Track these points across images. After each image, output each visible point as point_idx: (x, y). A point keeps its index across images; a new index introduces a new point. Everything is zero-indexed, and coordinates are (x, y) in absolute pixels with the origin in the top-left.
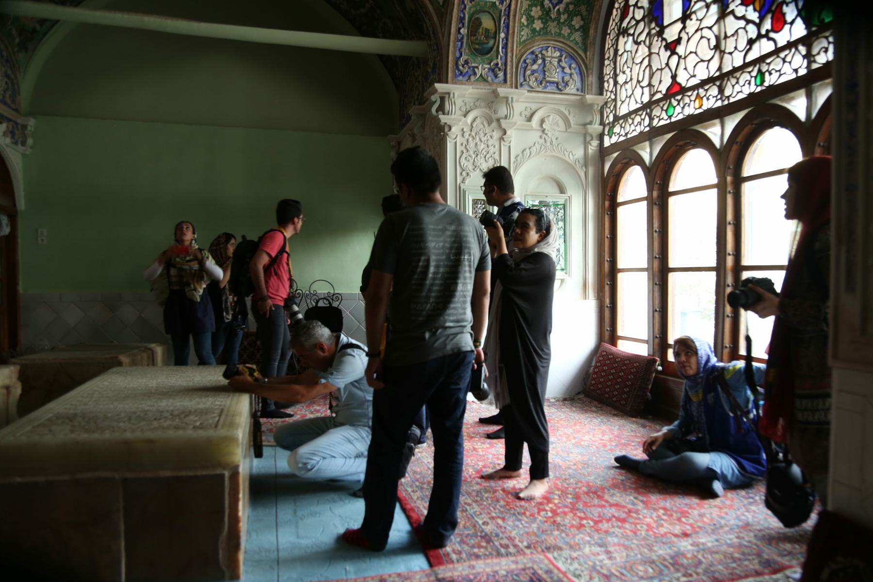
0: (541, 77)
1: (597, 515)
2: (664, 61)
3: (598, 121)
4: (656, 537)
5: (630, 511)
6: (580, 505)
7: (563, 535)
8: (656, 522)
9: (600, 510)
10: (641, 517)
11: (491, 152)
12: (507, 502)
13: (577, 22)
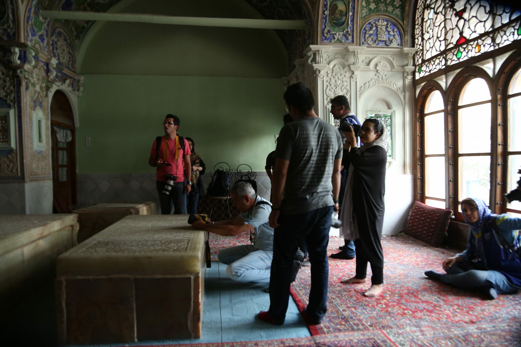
0: (375, 38)
1: (414, 307)
2: (455, 23)
3: (412, 64)
4: (452, 323)
5: (435, 306)
6: (403, 301)
7: (393, 319)
8: (452, 313)
10: (442, 309)
11: (345, 85)
12: (357, 298)
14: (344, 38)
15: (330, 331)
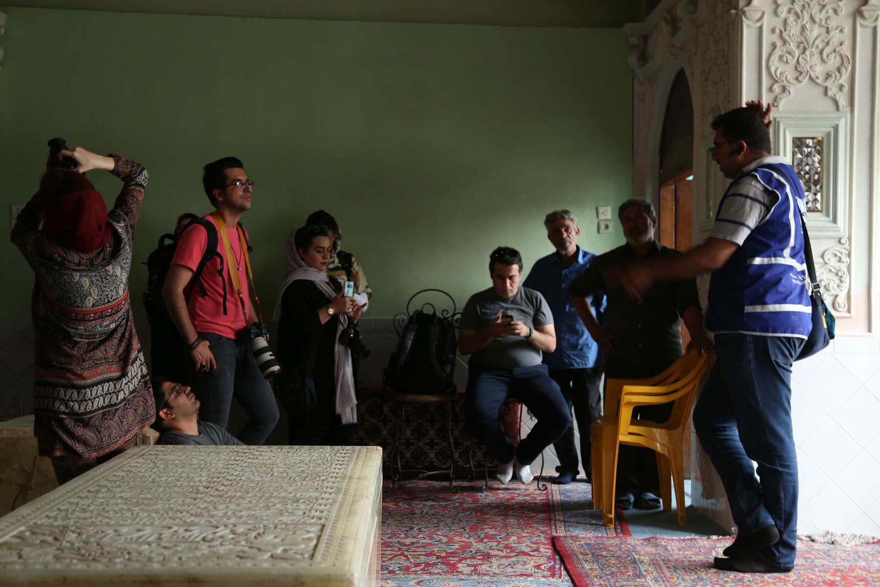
11: (835, 41)
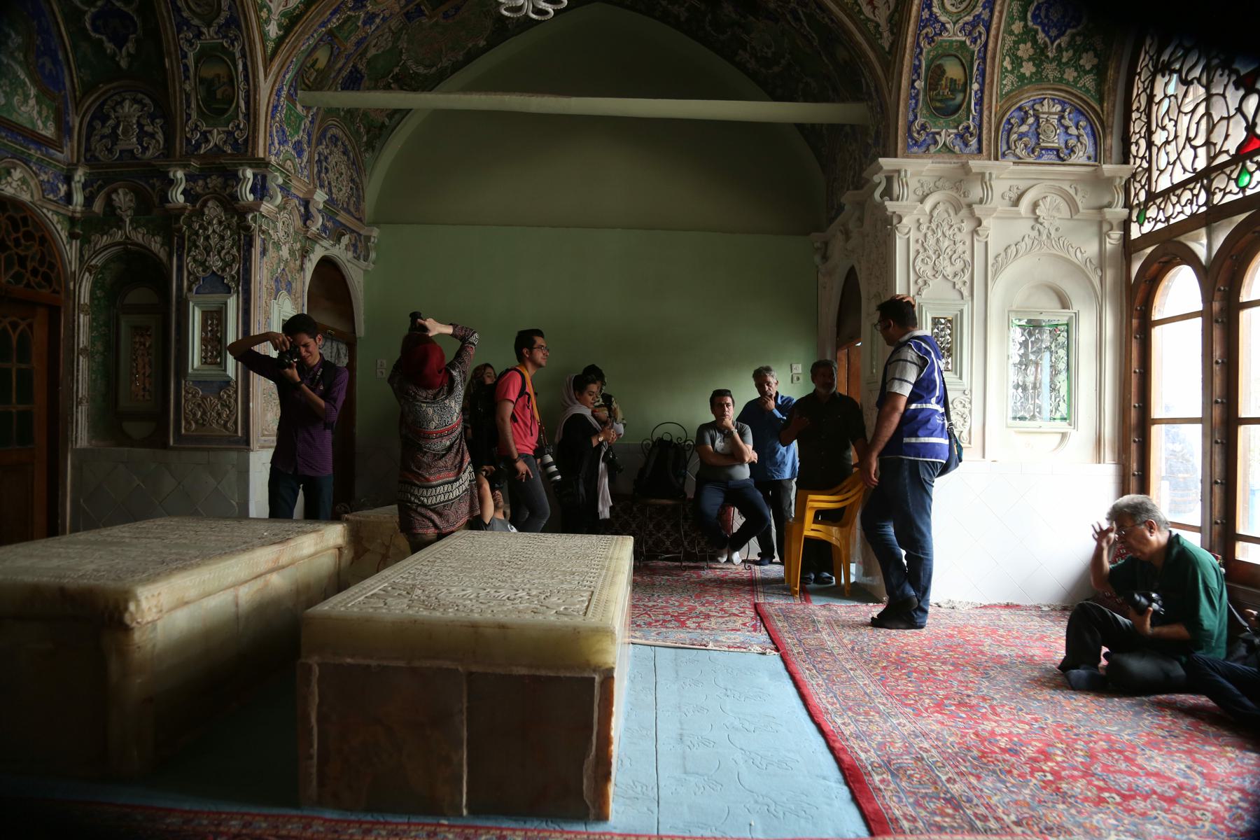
0: (1032, 143)
1: (1125, 786)
2: (1233, 105)
3: (1121, 202)
5: (1181, 787)
6: (1097, 768)
7: (1073, 811)
9: (1130, 779)
10: (1201, 798)
13: (1087, 61)
14: (959, 142)
15: (916, 828)
